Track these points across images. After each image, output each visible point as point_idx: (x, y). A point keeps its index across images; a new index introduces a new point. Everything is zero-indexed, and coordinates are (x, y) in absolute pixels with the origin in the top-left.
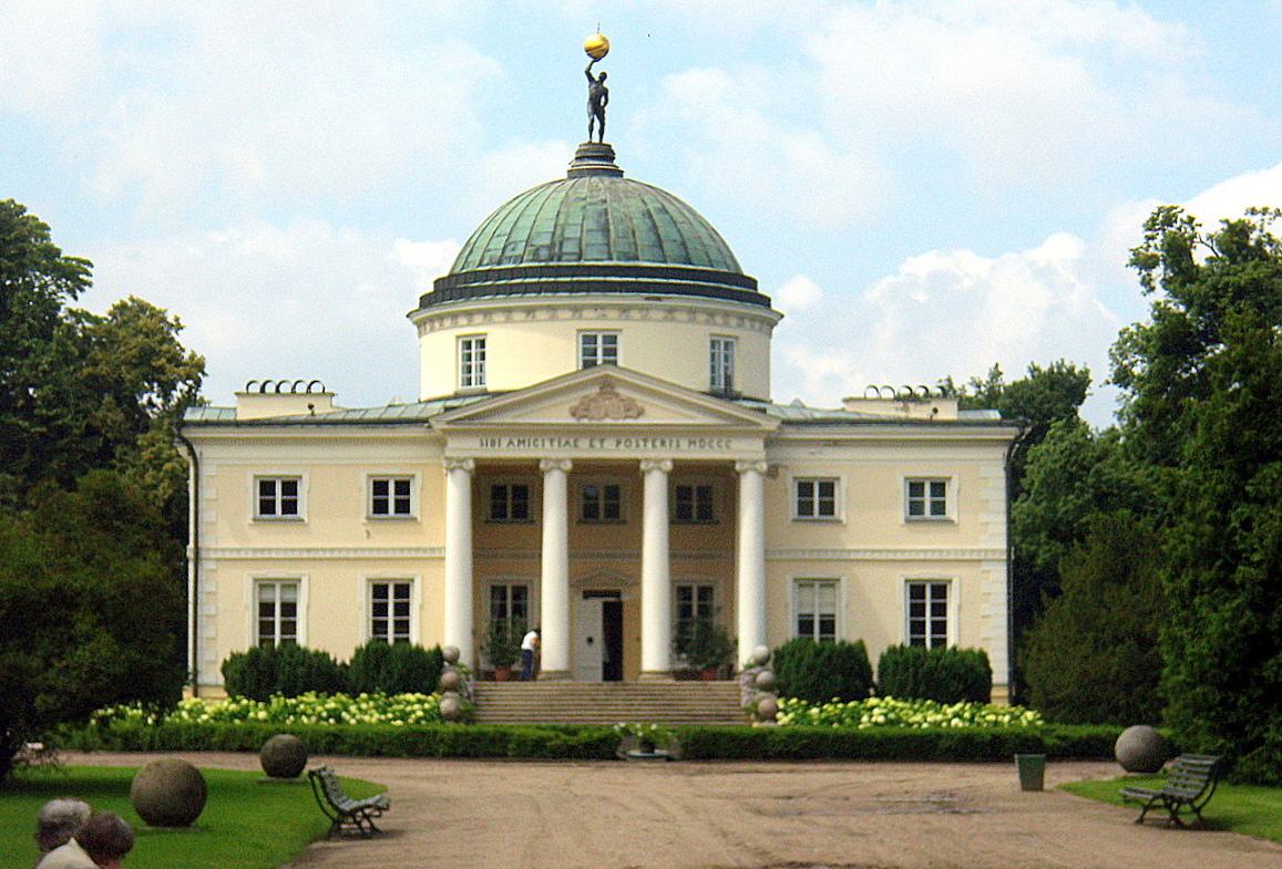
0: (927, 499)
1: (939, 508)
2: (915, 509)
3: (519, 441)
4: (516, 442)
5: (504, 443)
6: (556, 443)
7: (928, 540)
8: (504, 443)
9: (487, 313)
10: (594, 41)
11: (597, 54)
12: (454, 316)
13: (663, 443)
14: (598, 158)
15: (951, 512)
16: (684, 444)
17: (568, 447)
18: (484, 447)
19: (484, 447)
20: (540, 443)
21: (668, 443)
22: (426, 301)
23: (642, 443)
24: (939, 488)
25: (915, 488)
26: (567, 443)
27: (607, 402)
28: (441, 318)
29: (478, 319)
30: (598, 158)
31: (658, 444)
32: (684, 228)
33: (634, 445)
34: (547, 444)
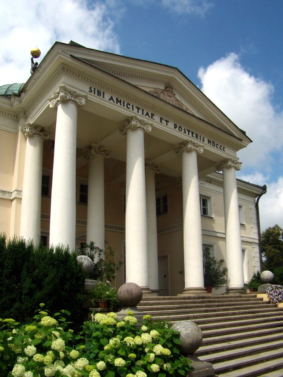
3: (117, 99)
4: (115, 100)
5: (107, 97)
6: (140, 111)
8: (107, 97)
10: (35, 49)
13: (197, 137)
16: (206, 141)
17: (147, 116)
18: (93, 93)
19: (93, 93)
20: (131, 107)
21: (199, 137)
23: (187, 132)
26: (147, 114)
27: (169, 98)
31: (194, 135)
33: (183, 131)
34: (135, 110)
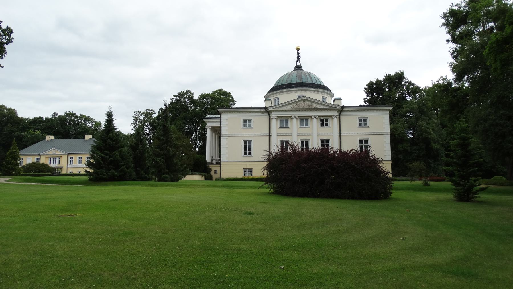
0: (363, 122)
1: (365, 124)
2: (360, 124)
7: (363, 130)
9: (279, 93)
11: (298, 49)
12: (273, 94)
14: (298, 68)
15: (368, 125)
22: (268, 93)
24: (365, 120)
25: (360, 120)
28: (271, 95)
29: (278, 94)
30: (298, 68)
32: (313, 78)
